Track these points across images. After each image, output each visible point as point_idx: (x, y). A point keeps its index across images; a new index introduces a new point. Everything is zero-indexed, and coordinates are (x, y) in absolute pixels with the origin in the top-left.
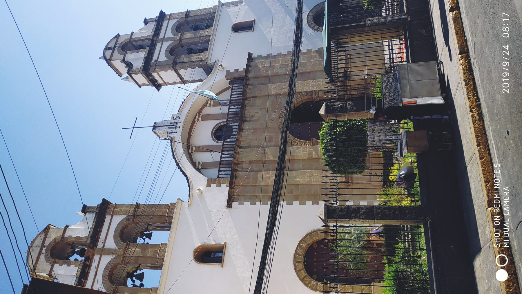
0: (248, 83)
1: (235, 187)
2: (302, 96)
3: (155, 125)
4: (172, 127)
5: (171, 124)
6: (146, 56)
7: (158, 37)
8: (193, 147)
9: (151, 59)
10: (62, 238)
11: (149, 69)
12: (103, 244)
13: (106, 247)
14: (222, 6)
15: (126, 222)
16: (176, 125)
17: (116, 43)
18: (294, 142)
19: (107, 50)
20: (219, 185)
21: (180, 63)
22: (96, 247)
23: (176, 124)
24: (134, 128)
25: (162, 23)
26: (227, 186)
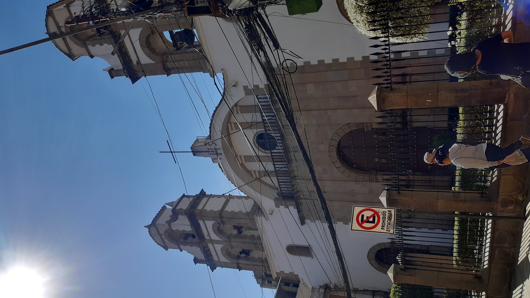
0: (278, 107)
8: (240, 156)
9: (131, 61)
11: (137, 76)
13: (212, 238)
15: (218, 225)
16: (217, 152)
17: (59, 27)
18: (351, 176)
21: (173, 68)
22: (206, 239)
24: (171, 152)
26: (294, 208)
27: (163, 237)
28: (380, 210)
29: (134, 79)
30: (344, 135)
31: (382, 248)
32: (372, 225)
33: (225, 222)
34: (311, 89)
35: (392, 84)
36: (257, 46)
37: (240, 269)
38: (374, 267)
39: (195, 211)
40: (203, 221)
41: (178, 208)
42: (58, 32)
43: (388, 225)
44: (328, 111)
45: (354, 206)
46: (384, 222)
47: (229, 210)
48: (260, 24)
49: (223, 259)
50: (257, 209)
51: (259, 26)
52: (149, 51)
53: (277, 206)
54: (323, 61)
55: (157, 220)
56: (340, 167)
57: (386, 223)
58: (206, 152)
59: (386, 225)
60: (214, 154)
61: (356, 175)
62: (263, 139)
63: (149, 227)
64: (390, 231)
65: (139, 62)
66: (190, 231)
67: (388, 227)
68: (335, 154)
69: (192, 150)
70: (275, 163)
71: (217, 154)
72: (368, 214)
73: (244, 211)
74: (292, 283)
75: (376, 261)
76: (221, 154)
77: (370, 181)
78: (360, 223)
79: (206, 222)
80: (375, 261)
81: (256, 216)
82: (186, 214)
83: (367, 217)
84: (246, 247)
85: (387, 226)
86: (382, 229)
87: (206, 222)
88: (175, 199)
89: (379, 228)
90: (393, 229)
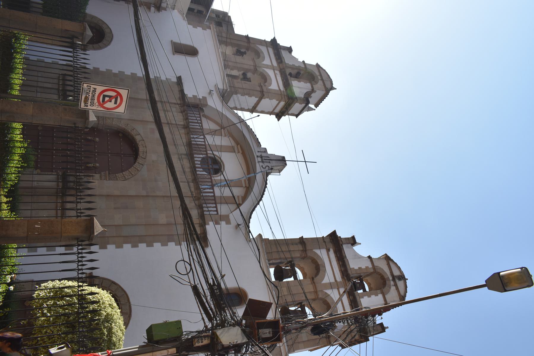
1: (178, 92)
2: (123, 176)
3: (284, 162)
4: (266, 158)
5: (269, 161)
6: (345, 260)
8: (239, 152)
9: (335, 252)
10: (311, 82)
12: (276, 72)
13: (272, 71)
15: (266, 84)
16: (262, 159)
17: (396, 285)
18: (125, 124)
19: (400, 275)
20: (194, 97)
21: (297, 244)
22: (279, 71)
23: (264, 161)
27: (319, 77)
28: (96, 107)
29: (333, 234)
30: (129, 168)
31: (97, 45)
32: (106, 93)
33: (259, 86)
34: (162, 219)
35: (77, 244)
36: (215, 288)
37: (247, 37)
38: (107, 25)
39: (288, 100)
40: (280, 90)
41: (303, 105)
42: (397, 281)
43: (89, 92)
44: (145, 194)
45: (124, 113)
46: (93, 96)
47: (253, 98)
48: (210, 311)
49: (263, 49)
50: (225, 96)
51: (211, 309)
52: (318, 261)
53: (204, 98)
54: (147, 246)
55: (324, 94)
56: (136, 135)
57: (90, 94)
58: (272, 160)
59: (91, 92)
61: (120, 125)
62: (215, 169)
63: (332, 88)
64: (87, 86)
65: (328, 250)
66: (294, 81)
67: (89, 90)
68: (141, 149)
69: (285, 162)
70: (204, 143)
71: (261, 157)
72: (110, 105)
73: (239, 95)
74: (195, 13)
75: (104, 30)
76: (258, 157)
77: (106, 118)
78: (119, 96)
79: (277, 88)
80: (105, 32)
81: (227, 90)
83: (111, 101)
84: (239, 59)
85: (90, 91)
86: (96, 89)
87: (277, 89)
88: (305, 114)
89: (100, 89)
90: (84, 87)
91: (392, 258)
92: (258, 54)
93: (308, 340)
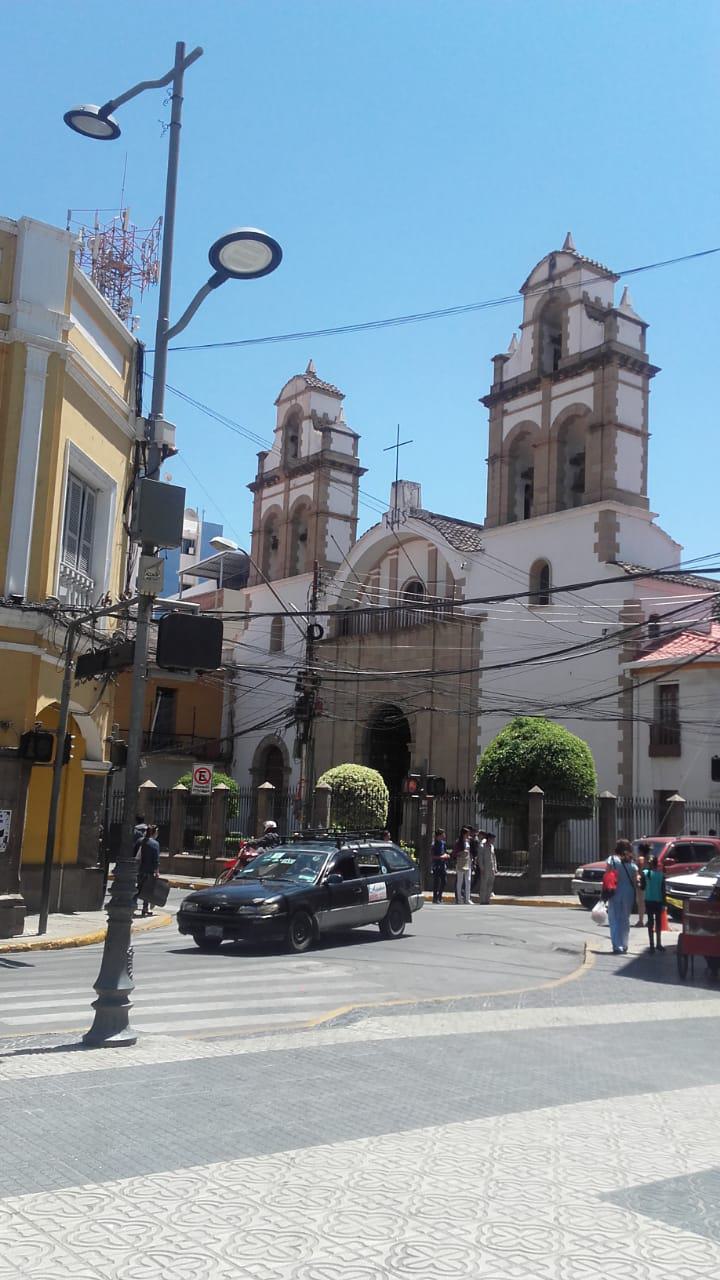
6: (521, 381)
7: (554, 384)
9: (508, 400)
14: (601, 512)
17: (563, 274)
25: (585, 371)
27: (294, 402)
29: (486, 401)
37: (253, 533)
41: (333, 435)
42: (556, 271)
47: (328, 527)
49: (266, 505)
60: (392, 519)
65: (505, 413)
72: (207, 775)
76: (392, 529)
82: (322, 452)
84: (281, 547)
89: (195, 783)
91: (525, 281)
92: (272, 516)
93: (602, 462)
